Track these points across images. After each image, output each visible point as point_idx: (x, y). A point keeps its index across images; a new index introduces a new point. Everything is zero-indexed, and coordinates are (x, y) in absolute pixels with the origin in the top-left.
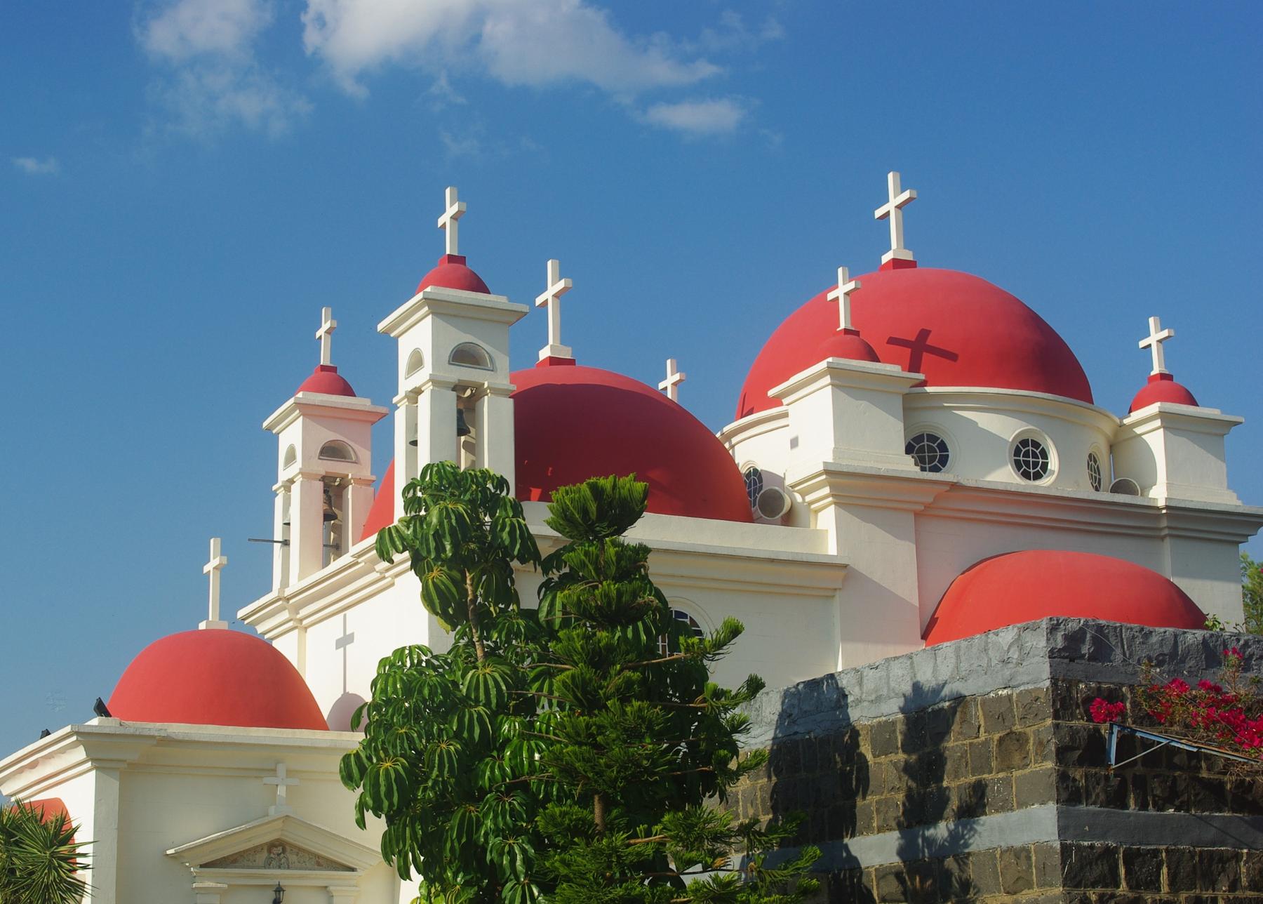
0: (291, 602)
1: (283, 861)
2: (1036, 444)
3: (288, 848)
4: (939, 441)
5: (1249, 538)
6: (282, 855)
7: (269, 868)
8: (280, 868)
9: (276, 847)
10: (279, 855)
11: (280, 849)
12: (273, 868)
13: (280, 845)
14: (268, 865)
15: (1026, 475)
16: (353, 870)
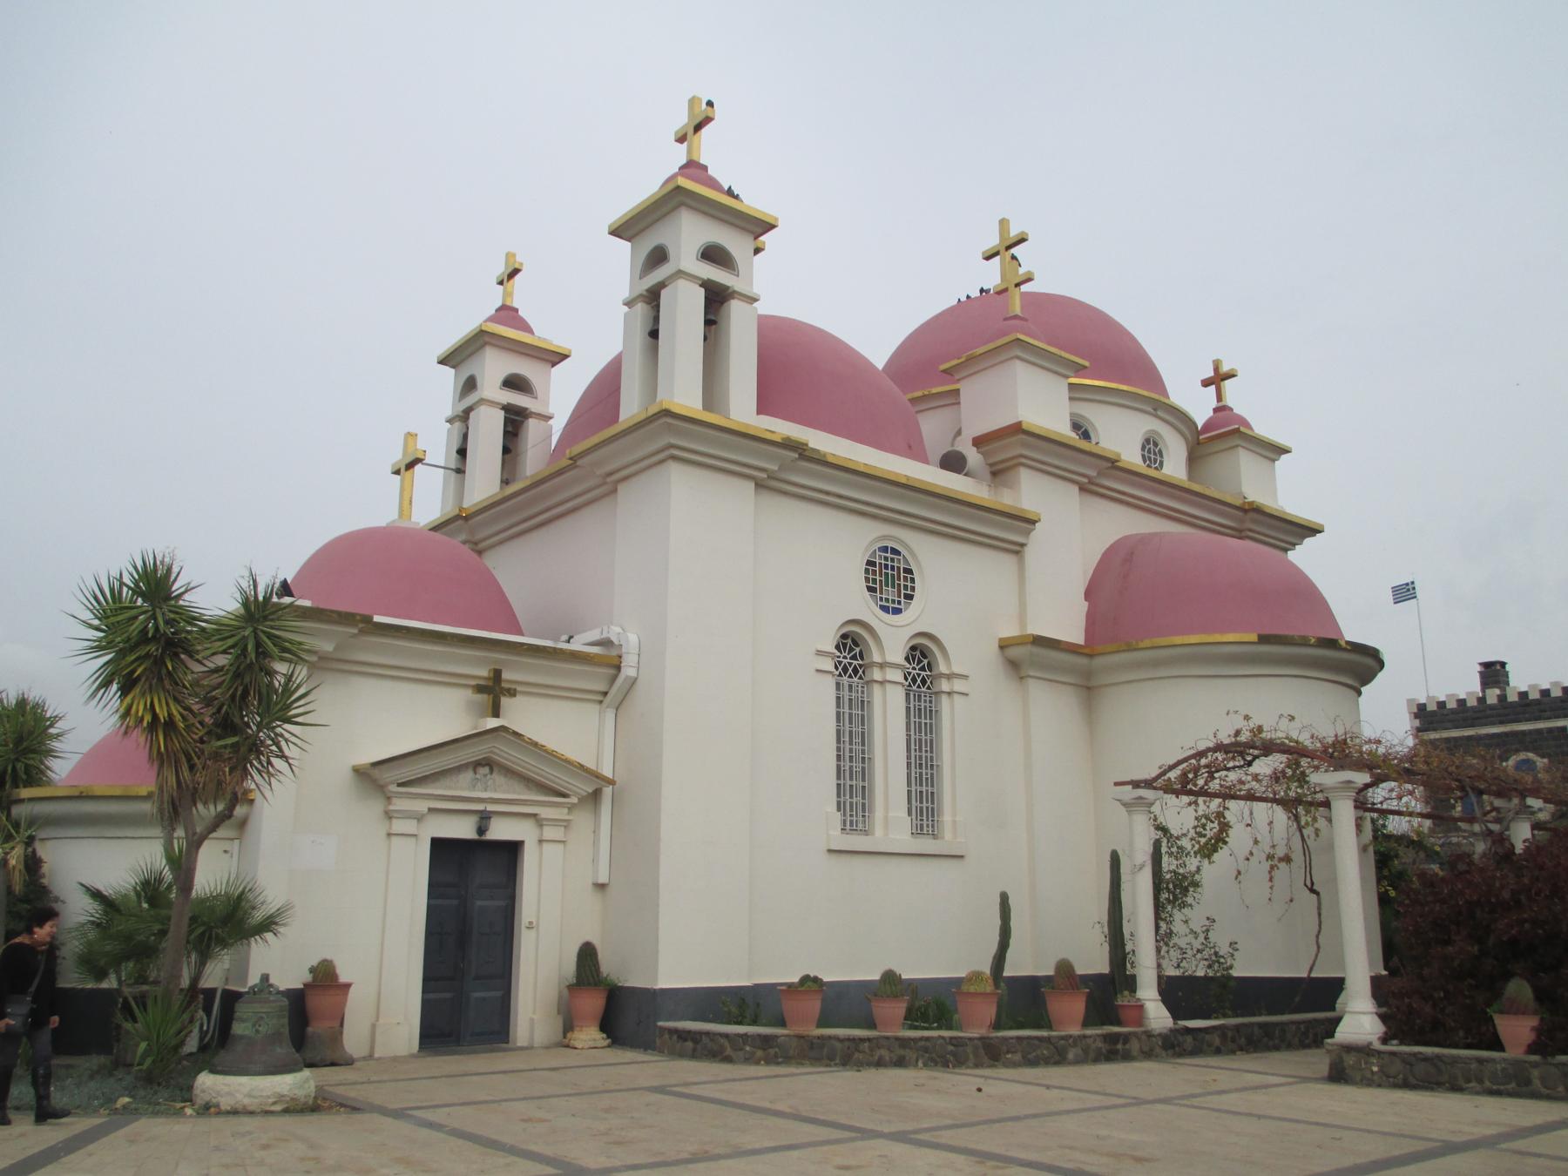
0: (470, 522)
1: (489, 783)
2: (1156, 444)
3: (495, 769)
4: (1083, 429)
5: (1297, 547)
6: (489, 776)
7: (474, 790)
8: (486, 790)
9: (484, 766)
10: (485, 776)
11: (486, 770)
12: (479, 790)
13: (487, 765)
14: (473, 787)
16: (564, 795)
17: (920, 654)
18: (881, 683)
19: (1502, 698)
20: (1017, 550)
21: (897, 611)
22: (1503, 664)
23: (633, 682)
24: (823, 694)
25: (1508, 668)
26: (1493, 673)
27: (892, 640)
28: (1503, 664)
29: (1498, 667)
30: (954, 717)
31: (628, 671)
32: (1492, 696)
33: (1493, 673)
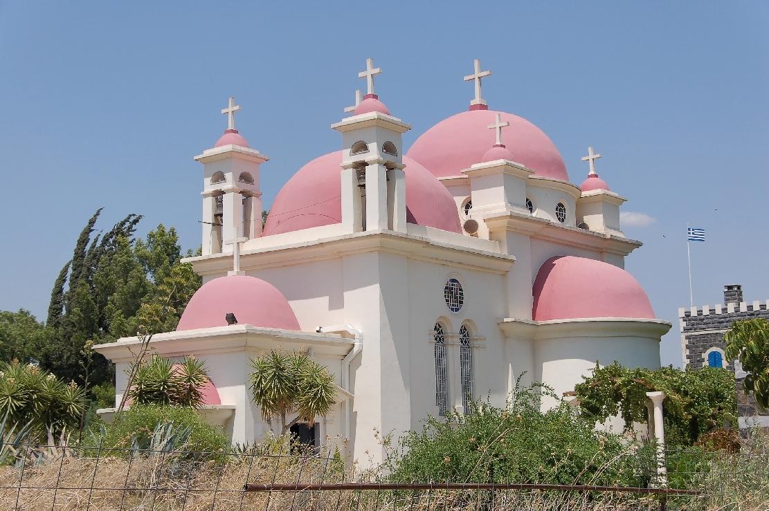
15: (559, 219)
17: (464, 330)
18: (451, 345)
19: (737, 310)
20: (505, 274)
21: (457, 310)
22: (739, 287)
23: (360, 353)
24: (429, 349)
25: (742, 289)
26: (733, 292)
27: (454, 325)
28: (739, 287)
29: (736, 289)
30: (477, 355)
31: (356, 349)
32: (731, 308)
33: (733, 292)
